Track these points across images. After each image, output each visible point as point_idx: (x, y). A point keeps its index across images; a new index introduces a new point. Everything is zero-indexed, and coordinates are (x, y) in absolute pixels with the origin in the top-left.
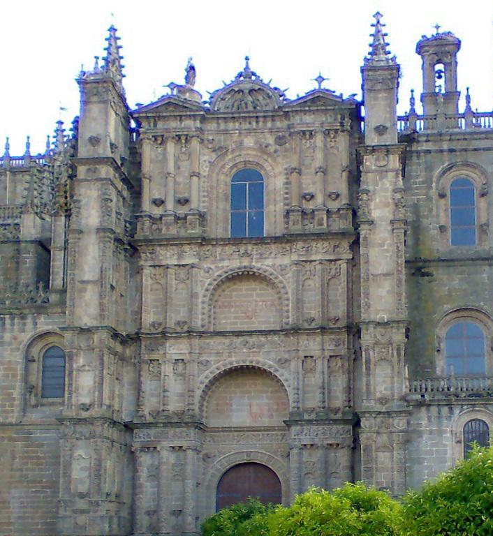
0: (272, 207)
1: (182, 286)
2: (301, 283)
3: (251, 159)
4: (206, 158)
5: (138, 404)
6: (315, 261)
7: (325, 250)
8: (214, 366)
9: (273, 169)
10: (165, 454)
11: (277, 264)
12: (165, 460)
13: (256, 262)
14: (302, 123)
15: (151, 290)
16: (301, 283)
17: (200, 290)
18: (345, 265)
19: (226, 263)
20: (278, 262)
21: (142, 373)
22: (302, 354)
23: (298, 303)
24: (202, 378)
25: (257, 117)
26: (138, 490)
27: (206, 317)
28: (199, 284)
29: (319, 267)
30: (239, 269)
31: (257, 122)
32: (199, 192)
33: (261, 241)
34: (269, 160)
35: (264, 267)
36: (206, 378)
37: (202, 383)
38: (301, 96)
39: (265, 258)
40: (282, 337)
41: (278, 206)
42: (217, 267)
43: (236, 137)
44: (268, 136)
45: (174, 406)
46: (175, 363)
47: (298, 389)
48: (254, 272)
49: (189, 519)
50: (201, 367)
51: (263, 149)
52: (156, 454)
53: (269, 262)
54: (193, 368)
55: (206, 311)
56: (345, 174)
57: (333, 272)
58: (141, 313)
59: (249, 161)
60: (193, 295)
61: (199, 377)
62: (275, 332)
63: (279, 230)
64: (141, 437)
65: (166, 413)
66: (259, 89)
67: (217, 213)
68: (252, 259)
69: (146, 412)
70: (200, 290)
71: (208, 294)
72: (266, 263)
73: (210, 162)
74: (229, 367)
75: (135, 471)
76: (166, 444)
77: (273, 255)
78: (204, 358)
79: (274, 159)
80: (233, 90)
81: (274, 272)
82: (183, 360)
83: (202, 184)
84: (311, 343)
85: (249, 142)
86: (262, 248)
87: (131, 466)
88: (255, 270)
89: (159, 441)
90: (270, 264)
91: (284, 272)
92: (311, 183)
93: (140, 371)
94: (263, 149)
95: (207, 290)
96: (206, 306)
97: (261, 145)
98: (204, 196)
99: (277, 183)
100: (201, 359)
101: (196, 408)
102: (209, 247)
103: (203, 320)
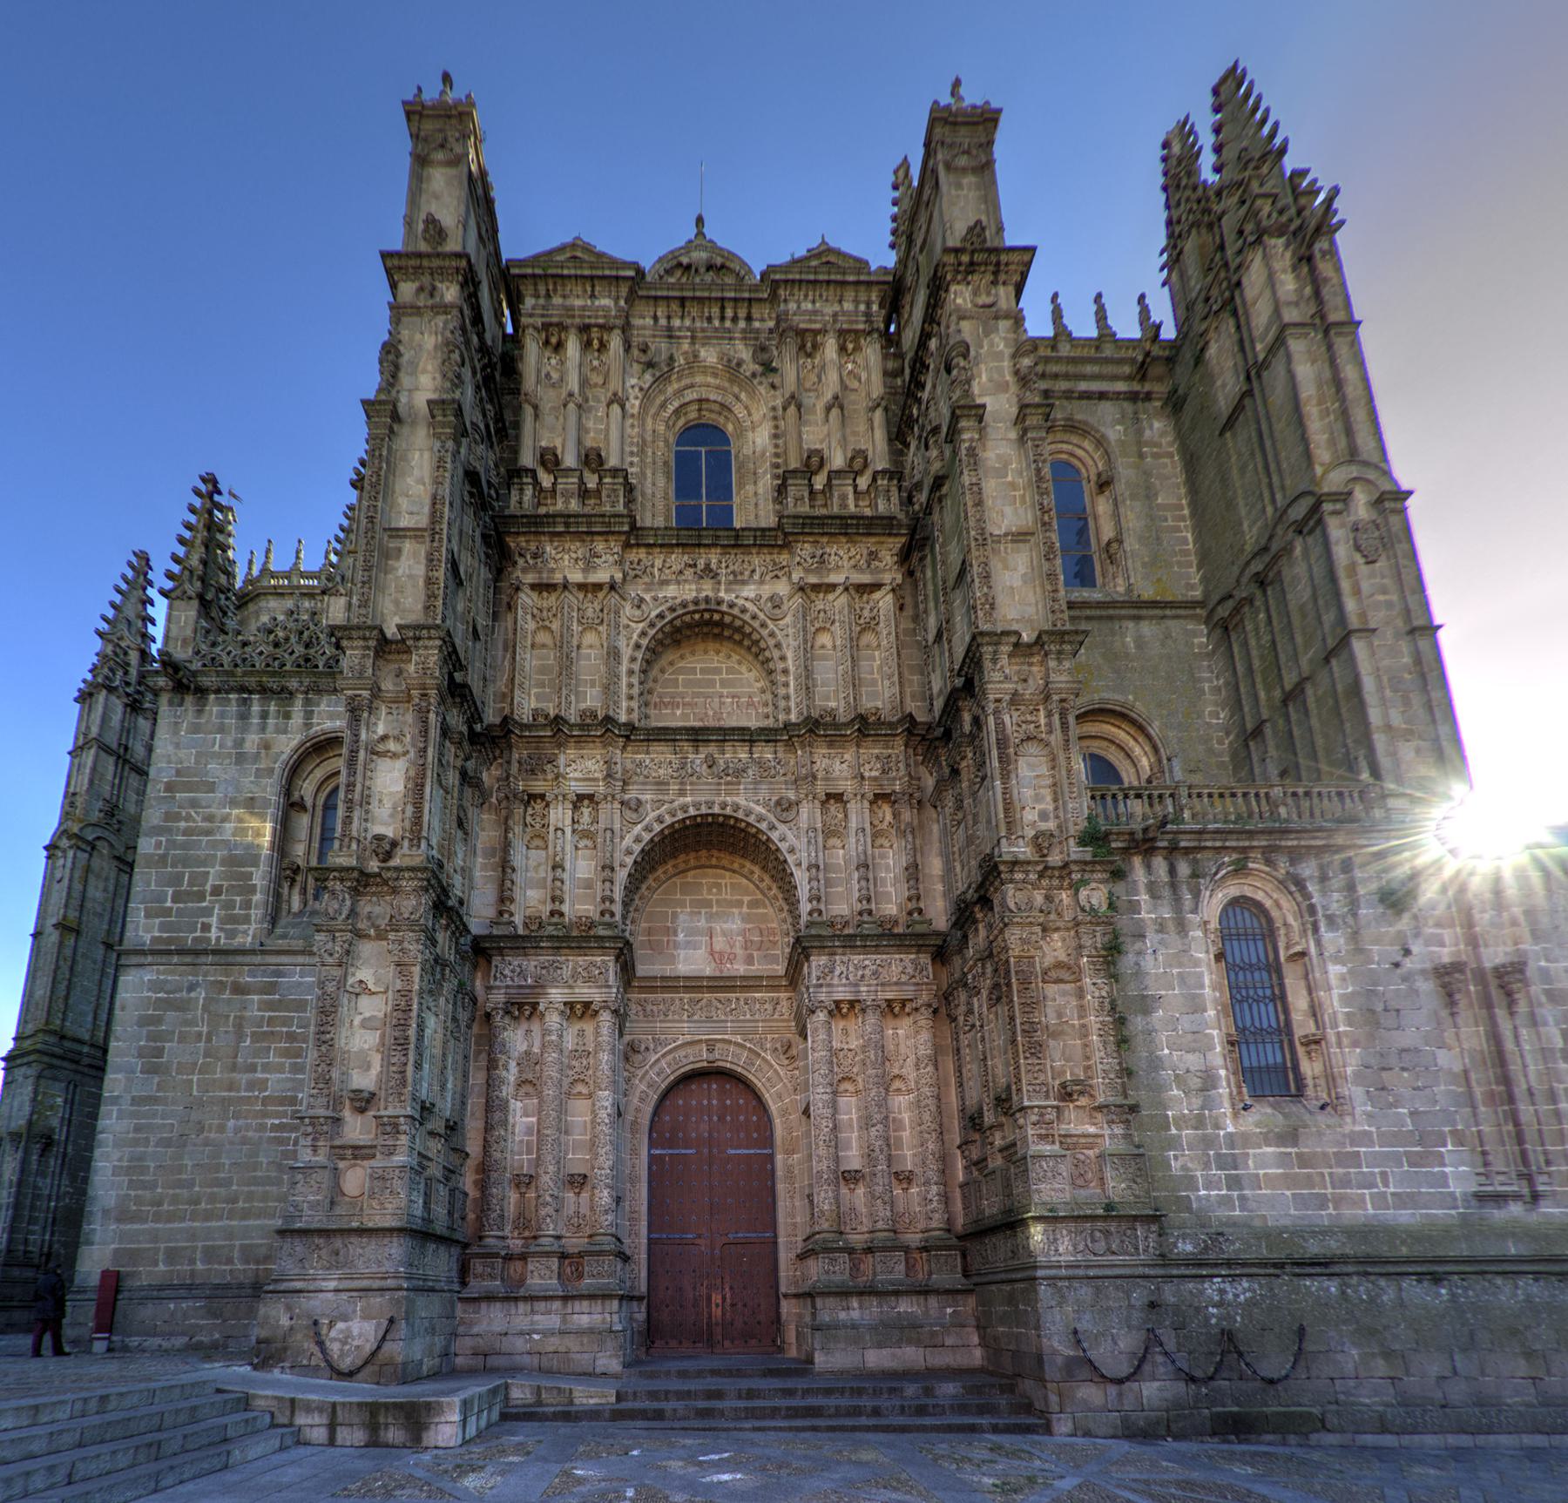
0: (750, 488)
1: (590, 638)
2: (809, 637)
3: (712, 397)
4: (634, 381)
5: (504, 898)
6: (832, 587)
7: (853, 562)
8: (652, 815)
9: (750, 414)
10: (553, 1019)
11: (765, 597)
12: (554, 1038)
13: (727, 591)
14: (798, 311)
15: (533, 646)
16: (809, 637)
17: (626, 652)
18: (890, 596)
19: (671, 591)
20: (767, 590)
21: (510, 823)
22: (820, 788)
23: (807, 677)
24: (628, 840)
25: (723, 299)
26: (497, 1116)
27: (634, 704)
28: (624, 632)
29: (844, 599)
30: (696, 602)
31: (723, 318)
32: (622, 443)
33: (738, 541)
34: (743, 396)
35: (740, 602)
36: (638, 840)
37: (629, 852)
38: (797, 256)
39: (744, 583)
40: (781, 748)
41: (761, 484)
42: (655, 599)
43: (686, 346)
44: (740, 345)
45: (579, 907)
46: (576, 807)
47: (818, 867)
48: (723, 613)
49: (605, 1197)
50: (629, 815)
51: (732, 368)
52: (536, 1027)
53: (749, 591)
54: (610, 814)
55: (635, 691)
56: (878, 415)
57: (866, 613)
58: (512, 691)
59: (707, 400)
60: (614, 654)
61: (622, 838)
62: (767, 735)
63: (768, 519)
64: (513, 970)
65: (555, 919)
66: (723, 266)
67: (653, 495)
68: (719, 583)
69: (518, 919)
70: (626, 652)
71: (639, 655)
72: (745, 594)
73: (641, 389)
74: (680, 816)
75: (492, 1065)
76: (557, 995)
77: (756, 577)
78: (630, 795)
79: (752, 394)
80: (680, 265)
81: (761, 616)
82: (591, 797)
83: (629, 430)
84: (837, 766)
85: (709, 355)
86: (736, 561)
87: (484, 1056)
88: (724, 608)
89: (543, 987)
90: (752, 595)
91: (777, 611)
92: (817, 434)
93: (507, 819)
94: (732, 368)
95: (638, 646)
96: (635, 680)
97: (729, 361)
98: (632, 453)
99: (759, 441)
100: (627, 797)
101: (617, 908)
102: (642, 553)
103: (630, 711)
